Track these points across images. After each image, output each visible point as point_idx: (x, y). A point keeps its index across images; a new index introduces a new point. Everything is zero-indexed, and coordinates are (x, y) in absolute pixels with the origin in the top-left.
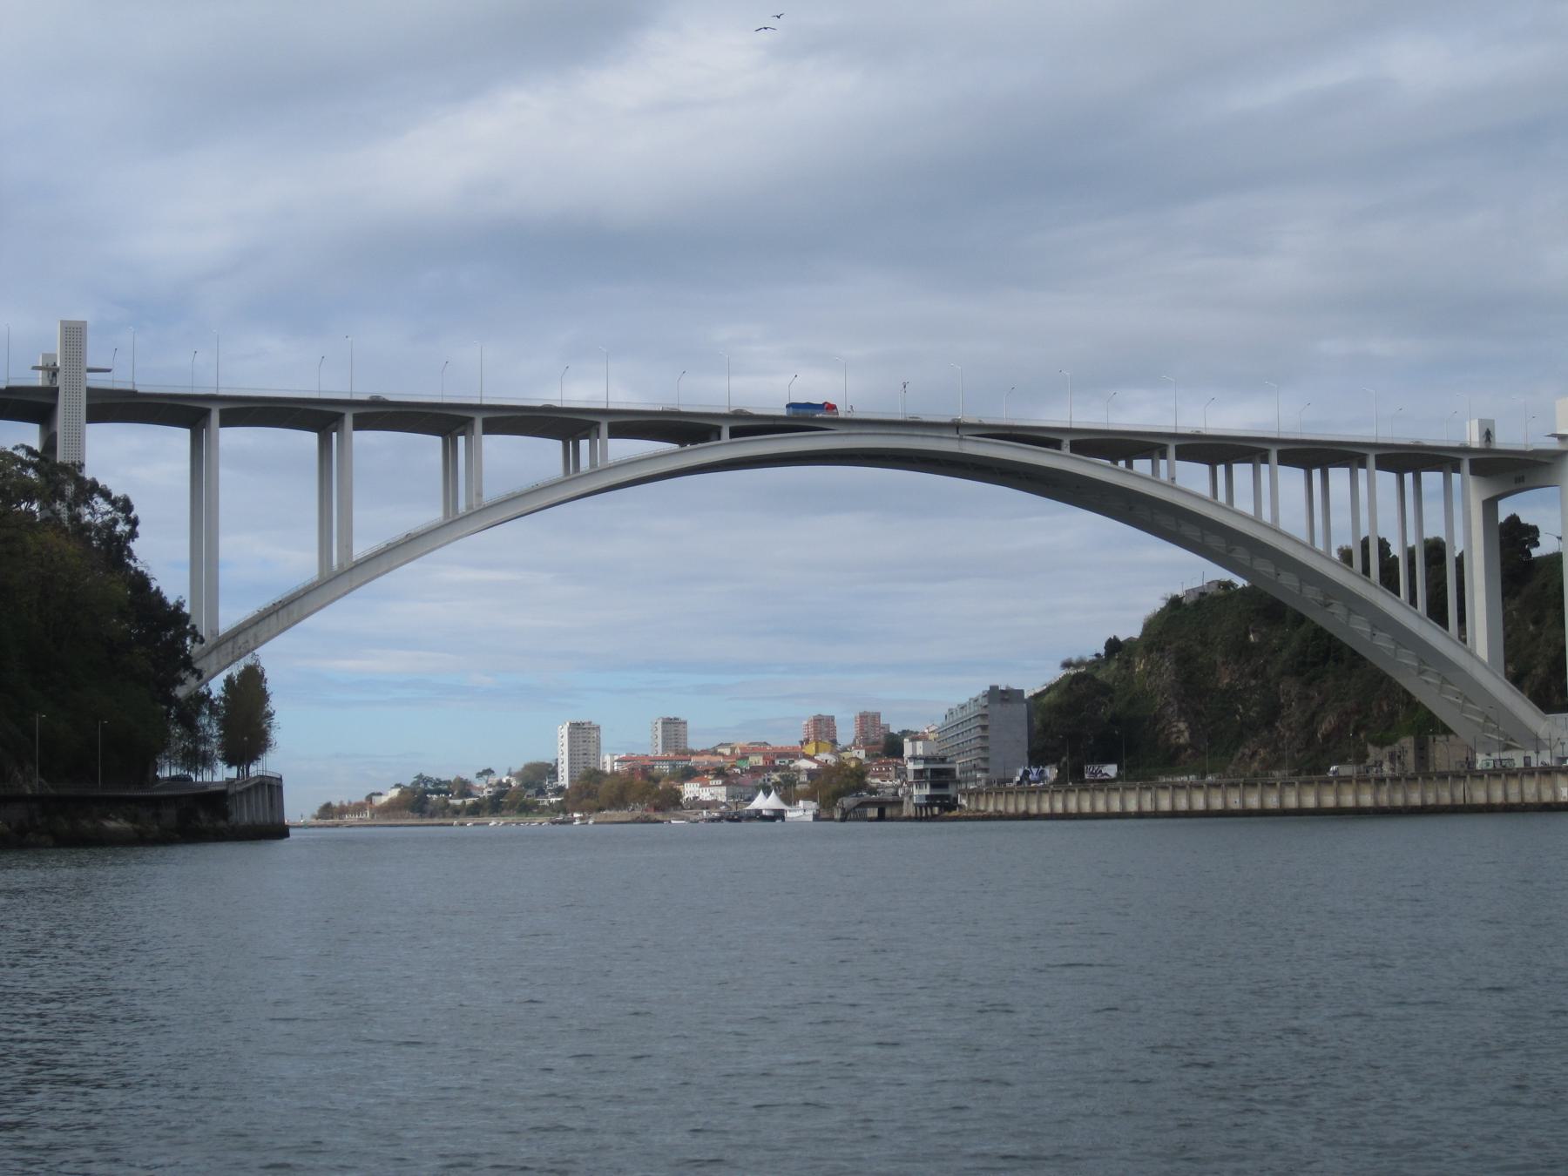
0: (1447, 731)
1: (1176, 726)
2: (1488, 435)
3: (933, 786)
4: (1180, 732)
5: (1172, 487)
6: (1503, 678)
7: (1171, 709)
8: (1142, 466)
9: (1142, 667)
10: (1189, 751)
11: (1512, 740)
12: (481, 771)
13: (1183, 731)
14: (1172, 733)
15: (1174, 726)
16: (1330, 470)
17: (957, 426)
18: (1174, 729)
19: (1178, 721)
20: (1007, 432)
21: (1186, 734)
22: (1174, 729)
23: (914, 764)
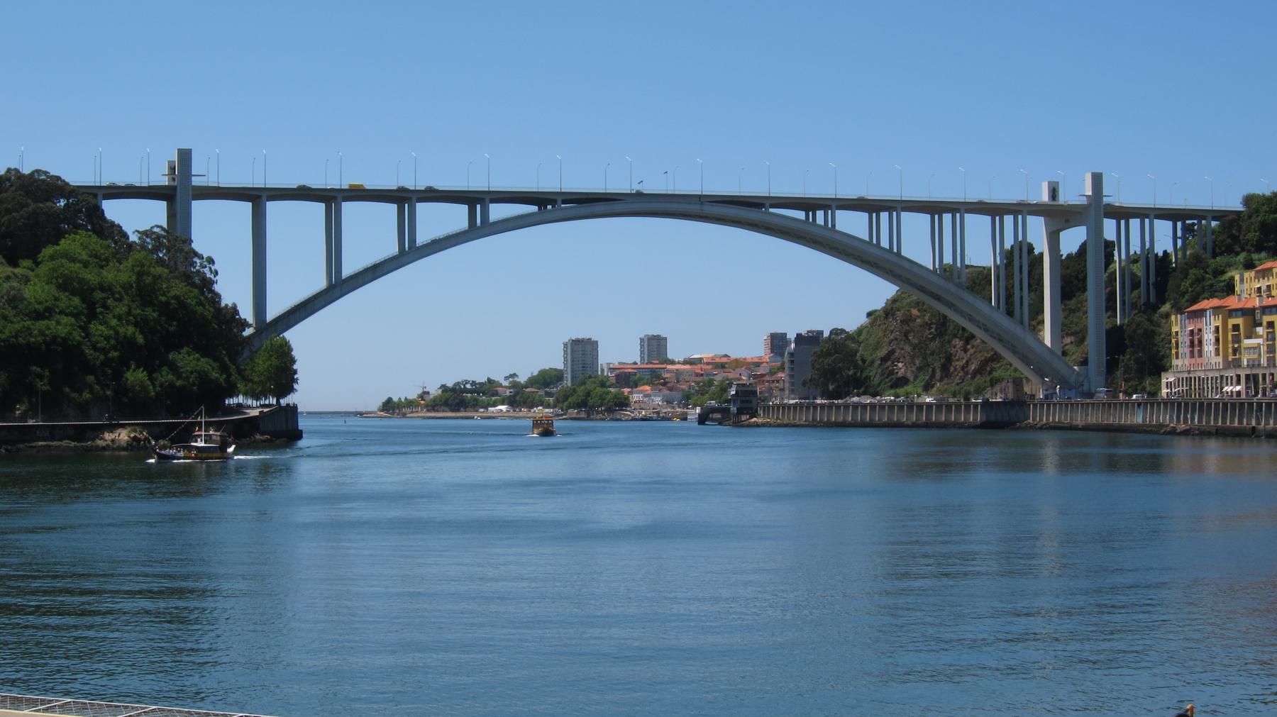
2: (1054, 193)
8: (820, 214)
12: (508, 375)
14: (894, 370)
16: (944, 215)
21: (903, 370)
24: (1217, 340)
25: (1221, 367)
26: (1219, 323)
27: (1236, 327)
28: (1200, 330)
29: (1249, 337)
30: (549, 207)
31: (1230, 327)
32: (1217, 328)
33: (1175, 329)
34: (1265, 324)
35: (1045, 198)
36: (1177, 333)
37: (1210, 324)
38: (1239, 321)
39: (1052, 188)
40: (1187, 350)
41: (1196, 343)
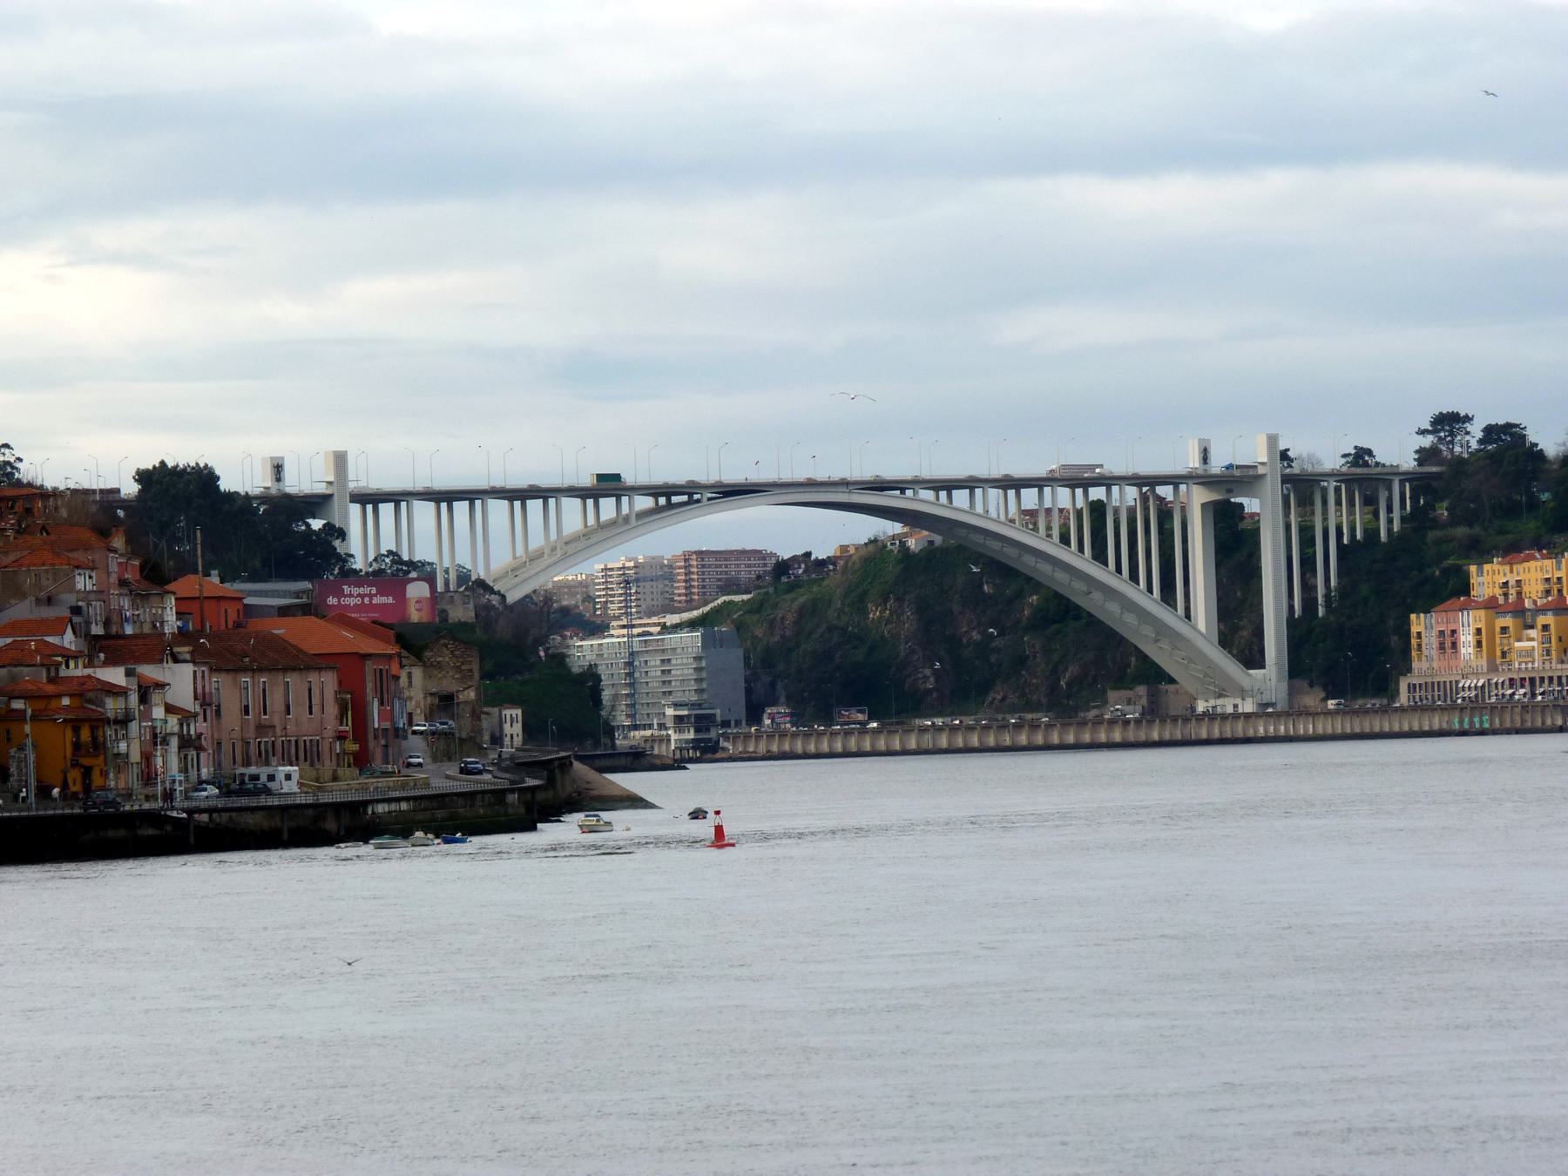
0: (1172, 681)
1: (922, 672)
3: (697, 731)
4: (926, 678)
5: (987, 518)
6: (1217, 645)
7: (916, 657)
8: (961, 497)
9: (878, 613)
10: (935, 695)
11: (1224, 690)
13: (929, 677)
14: (918, 679)
15: (919, 672)
17: (845, 483)
18: (920, 675)
19: (924, 667)
20: (878, 485)
21: (932, 679)
22: (920, 675)
23: (675, 710)
24: (1479, 644)
25: (1486, 671)
26: (1481, 625)
27: (1504, 630)
28: (1454, 632)
29: (1519, 640)
30: (675, 499)
31: (1498, 630)
32: (1479, 631)
33: (1414, 629)
34: (1539, 627)
35: (1194, 462)
36: (1419, 634)
37: (1469, 626)
38: (1507, 621)
39: (1202, 449)
40: (1435, 653)
41: (1449, 643)
